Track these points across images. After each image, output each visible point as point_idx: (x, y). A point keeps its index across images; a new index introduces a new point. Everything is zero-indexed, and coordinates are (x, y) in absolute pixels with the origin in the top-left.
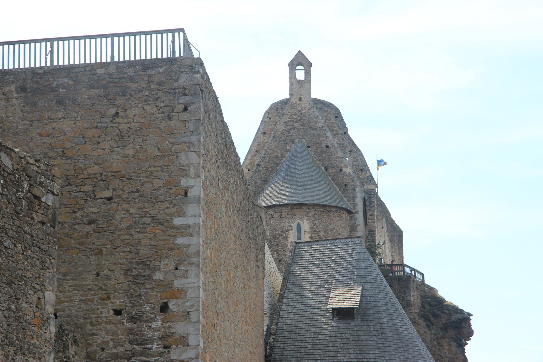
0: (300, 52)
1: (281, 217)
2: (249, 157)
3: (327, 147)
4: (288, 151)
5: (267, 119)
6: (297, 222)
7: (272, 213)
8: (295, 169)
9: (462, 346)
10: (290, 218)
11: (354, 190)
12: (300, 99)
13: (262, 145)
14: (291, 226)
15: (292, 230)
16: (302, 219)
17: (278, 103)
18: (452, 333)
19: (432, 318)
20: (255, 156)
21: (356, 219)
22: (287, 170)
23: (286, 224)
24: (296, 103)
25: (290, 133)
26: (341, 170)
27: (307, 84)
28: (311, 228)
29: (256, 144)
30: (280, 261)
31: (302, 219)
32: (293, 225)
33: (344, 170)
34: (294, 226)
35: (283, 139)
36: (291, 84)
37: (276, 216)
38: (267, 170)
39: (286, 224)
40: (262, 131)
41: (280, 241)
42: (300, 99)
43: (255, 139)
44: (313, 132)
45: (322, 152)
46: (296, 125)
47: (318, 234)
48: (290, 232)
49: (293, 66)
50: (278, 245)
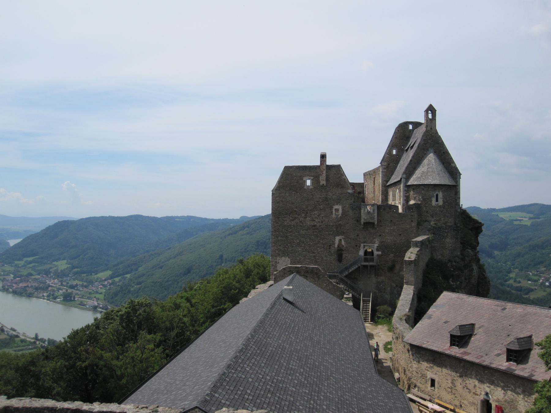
2: (389, 148)
3: (444, 153)
5: (397, 131)
6: (436, 193)
7: (424, 188)
9: (477, 236)
11: (456, 175)
12: (431, 129)
13: (394, 143)
14: (433, 195)
15: (434, 197)
16: (439, 192)
20: (391, 148)
24: (429, 130)
25: (426, 145)
26: (450, 164)
27: (434, 121)
28: (443, 196)
29: (392, 143)
30: (427, 212)
33: (452, 164)
34: (435, 195)
36: (427, 121)
38: (415, 163)
40: (394, 137)
42: (431, 129)
43: (391, 140)
46: (429, 141)
48: (433, 198)
49: (427, 111)
50: (426, 204)
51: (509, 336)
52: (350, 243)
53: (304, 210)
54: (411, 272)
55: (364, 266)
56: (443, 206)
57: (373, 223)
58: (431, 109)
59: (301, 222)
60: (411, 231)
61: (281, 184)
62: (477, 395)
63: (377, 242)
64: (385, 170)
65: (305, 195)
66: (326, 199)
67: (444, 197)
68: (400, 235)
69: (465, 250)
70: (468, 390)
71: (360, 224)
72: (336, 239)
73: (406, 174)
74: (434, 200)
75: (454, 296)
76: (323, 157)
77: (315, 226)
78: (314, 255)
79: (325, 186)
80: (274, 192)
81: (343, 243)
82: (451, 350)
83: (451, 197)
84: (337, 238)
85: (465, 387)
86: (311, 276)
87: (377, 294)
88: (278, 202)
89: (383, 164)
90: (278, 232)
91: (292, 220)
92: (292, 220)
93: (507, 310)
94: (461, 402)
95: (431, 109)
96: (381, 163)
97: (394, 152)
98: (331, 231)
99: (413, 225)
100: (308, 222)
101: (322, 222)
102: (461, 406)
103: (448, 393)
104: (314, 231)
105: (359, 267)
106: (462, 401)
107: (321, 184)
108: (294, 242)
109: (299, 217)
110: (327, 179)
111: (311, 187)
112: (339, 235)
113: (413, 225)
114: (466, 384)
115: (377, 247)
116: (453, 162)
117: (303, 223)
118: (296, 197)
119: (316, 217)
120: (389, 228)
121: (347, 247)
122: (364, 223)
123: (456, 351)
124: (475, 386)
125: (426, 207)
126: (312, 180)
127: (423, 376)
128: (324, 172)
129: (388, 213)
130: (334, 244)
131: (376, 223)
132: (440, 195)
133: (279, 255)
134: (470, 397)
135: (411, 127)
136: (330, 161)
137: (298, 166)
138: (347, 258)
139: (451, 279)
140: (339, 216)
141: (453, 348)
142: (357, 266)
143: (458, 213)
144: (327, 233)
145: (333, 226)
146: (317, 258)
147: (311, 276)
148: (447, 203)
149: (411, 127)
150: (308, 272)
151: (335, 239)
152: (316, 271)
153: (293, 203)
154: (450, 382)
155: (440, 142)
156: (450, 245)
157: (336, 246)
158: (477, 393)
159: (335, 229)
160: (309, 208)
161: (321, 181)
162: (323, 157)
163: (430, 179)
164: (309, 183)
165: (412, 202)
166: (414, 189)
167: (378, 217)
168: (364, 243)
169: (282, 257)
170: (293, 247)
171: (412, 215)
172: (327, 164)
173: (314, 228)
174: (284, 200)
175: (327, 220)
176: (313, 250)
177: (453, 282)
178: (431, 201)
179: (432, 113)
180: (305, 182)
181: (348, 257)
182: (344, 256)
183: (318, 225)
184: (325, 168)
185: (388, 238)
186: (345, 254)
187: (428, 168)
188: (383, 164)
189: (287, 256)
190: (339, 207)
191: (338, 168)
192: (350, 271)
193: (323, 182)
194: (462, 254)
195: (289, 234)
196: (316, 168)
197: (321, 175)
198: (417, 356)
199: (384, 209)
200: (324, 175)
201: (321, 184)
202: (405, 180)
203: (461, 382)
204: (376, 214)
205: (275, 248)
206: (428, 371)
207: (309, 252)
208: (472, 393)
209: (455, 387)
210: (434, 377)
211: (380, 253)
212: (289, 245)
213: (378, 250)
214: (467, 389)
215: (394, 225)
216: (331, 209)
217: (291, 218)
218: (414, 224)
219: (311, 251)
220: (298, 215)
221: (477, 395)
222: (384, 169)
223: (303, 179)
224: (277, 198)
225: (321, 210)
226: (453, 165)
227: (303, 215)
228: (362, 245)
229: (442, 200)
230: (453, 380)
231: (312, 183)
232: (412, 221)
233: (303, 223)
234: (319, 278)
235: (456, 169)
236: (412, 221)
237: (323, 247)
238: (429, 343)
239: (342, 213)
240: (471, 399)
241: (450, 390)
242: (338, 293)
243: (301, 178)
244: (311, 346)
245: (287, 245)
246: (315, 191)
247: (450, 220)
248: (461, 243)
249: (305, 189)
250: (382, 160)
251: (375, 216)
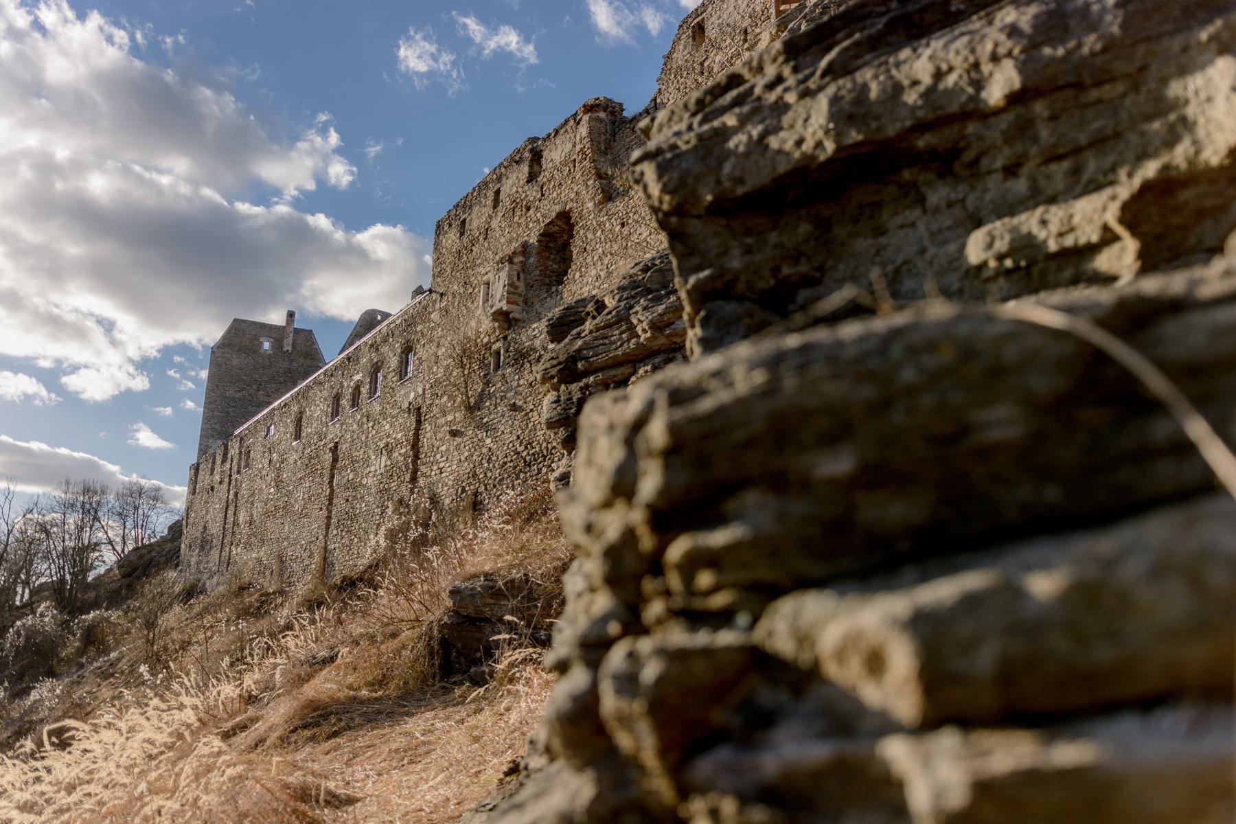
0: (421, 286)
59: (250, 395)
65: (260, 361)
66: (290, 371)
80: (215, 350)
88: (220, 365)
107: (285, 349)
111: (269, 352)
118: (246, 362)
128: (291, 335)
133: (213, 436)
135: (379, 318)
149: (379, 318)
153: (240, 369)
160: (265, 378)
162: (291, 315)
164: (267, 345)
174: (228, 362)
180: (262, 343)
184: (292, 330)
193: (288, 347)
195: (231, 410)
197: (286, 338)
200: (291, 338)
201: (285, 349)
205: (208, 426)
212: (229, 424)
217: (236, 389)
220: (248, 386)
224: (219, 359)
227: (255, 387)
231: (272, 347)
243: (256, 338)
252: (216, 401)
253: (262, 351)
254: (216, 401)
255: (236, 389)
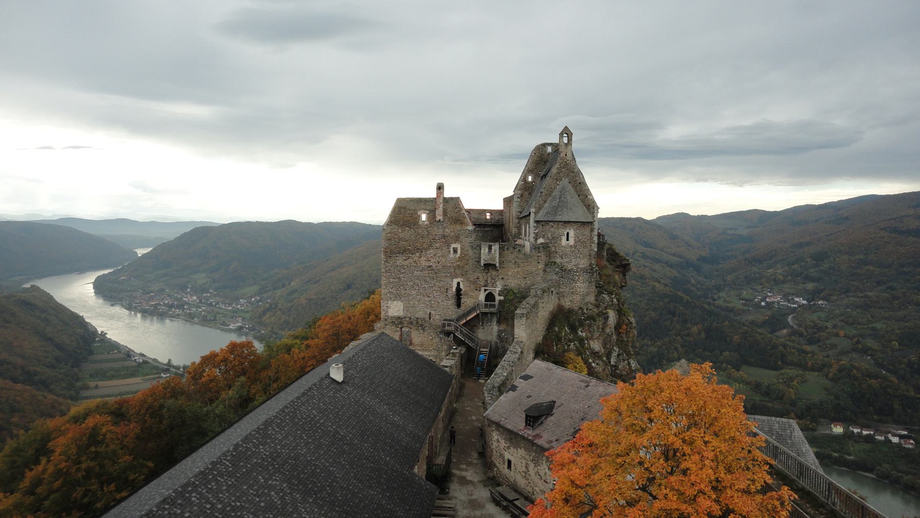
1: (558, 228)
2: (524, 174)
3: (580, 183)
4: (558, 184)
6: (567, 231)
8: (565, 198)
10: (563, 229)
16: (570, 230)
17: (540, 145)
18: (621, 269)
19: (611, 261)
21: (594, 225)
22: (560, 198)
23: (561, 232)
31: (570, 230)
32: (565, 233)
33: (588, 197)
34: (565, 233)
35: (556, 177)
37: (555, 226)
39: (561, 231)
41: (557, 241)
42: (566, 155)
44: (572, 174)
45: (577, 186)
46: (563, 170)
47: (578, 238)
49: (561, 135)
51: (583, 419)
52: (469, 287)
53: (418, 249)
54: (522, 326)
55: (485, 314)
56: (575, 247)
57: (494, 265)
58: (566, 132)
59: (415, 262)
60: (537, 274)
61: (393, 218)
62: (547, 482)
63: (498, 286)
64: (519, 200)
65: (420, 231)
66: (444, 236)
67: (576, 236)
68: (525, 278)
69: (600, 295)
70: (539, 477)
71: (480, 265)
72: (454, 282)
73: (536, 208)
74: (564, 238)
75: (544, 366)
76: (440, 188)
77: (430, 266)
78: (430, 299)
79: (442, 222)
81: (461, 286)
82: (525, 431)
83: (585, 235)
84: (455, 281)
85: (537, 473)
86: (415, 328)
87: (498, 344)
89: (516, 192)
90: (389, 273)
91: (406, 260)
92: (406, 260)
93: (589, 388)
94: (533, 488)
95: (566, 132)
96: (514, 191)
97: (530, 179)
98: (448, 273)
99: (539, 267)
100: (423, 262)
101: (438, 263)
102: (533, 492)
103: (523, 478)
104: (430, 272)
105: (478, 315)
106: (535, 488)
108: (407, 285)
109: (413, 256)
110: (445, 213)
112: (457, 277)
113: (539, 267)
114: (538, 469)
115: (499, 291)
116: (591, 194)
117: (417, 264)
118: (409, 234)
119: (432, 257)
120: (513, 270)
121: (465, 291)
122: (484, 264)
123: (529, 433)
124: (545, 474)
125: (555, 246)
126: (428, 214)
127: (502, 456)
128: (441, 206)
129: (512, 253)
130: (452, 288)
131: (497, 265)
132: (572, 234)
134: (541, 485)
136: (447, 194)
137: (412, 198)
138: (465, 303)
139: (580, 330)
140: (457, 256)
141: (528, 428)
142: (475, 314)
143: (594, 253)
144: (444, 274)
145: (450, 267)
146: (433, 302)
147: (415, 328)
148: (579, 243)
150: (411, 323)
151: (452, 282)
152: (420, 323)
154: (524, 465)
155: (576, 170)
156: (582, 290)
157: (454, 289)
158: (547, 481)
159: (453, 271)
161: (437, 216)
162: (440, 188)
163: (560, 215)
164: (424, 217)
165: (541, 241)
166: (543, 225)
167: (500, 257)
168: (485, 287)
169: (393, 301)
170: (406, 290)
171: (538, 256)
172: (445, 196)
173: (429, 269)
175: (444, 260)
176: (428, 294)
177: (582, 332)
178: (561, 240)
179: (568, 137)
180: (420, 216)
181: (467, 302)
182: (462, 300)
183: (434, 265)
184: (441, 201)
185: (512, 281)
186: (464, 298)
187: (559, 202)
188: (516, 192)
189: (400, 300)
190: (457, 246)
191: (457, 200)
192: (468, 319)
194: (596, 300)
195: (401, 276)
196: (432, 201)
198: (498, 433)
199: (508, 249)
202: (534, 214)
203: (533, 466)
204: (497, 255)
206: (506, 451)
207: (424, 296)
208: (543, 481)
209: (528, 471)
210: (512, 458)
211: (502, 298)
212: (402, 287)
213: (500, 295)
214: (539, 475)
215: (519, 267)
216: (448, 248)
217: (404, 258)
218: (541, 266)
219: (427, 295)
221: (547, 482)
222: (518, 198)
223: (417, 213)
224: (389, 235)
225: (437, 248)
226: (591, 198)
228: (483, 289)
229: (574, 239)
230: (527, 464)
231: (428, 218)
232: (539, 263)
233: (417, 264)
234: (423, 329)
235: (594, 202)
236: (539, 263)
237: (440, 291)
238: (506, 421)
239: (461, 252)
240: (542, 487)
241: (523, 474)
242: (446, 347)
243: (415, 212)
244: (384, 420)
245: (400, 288)
246: (431, 227)
247: (583, 261)
248: (596, 287)
249: (419, 225)
250: (515, 188)
251: (496, 257)
252: (390, 270)
253: (420, 223)
254: (390, 270)
255: (404, 258)
